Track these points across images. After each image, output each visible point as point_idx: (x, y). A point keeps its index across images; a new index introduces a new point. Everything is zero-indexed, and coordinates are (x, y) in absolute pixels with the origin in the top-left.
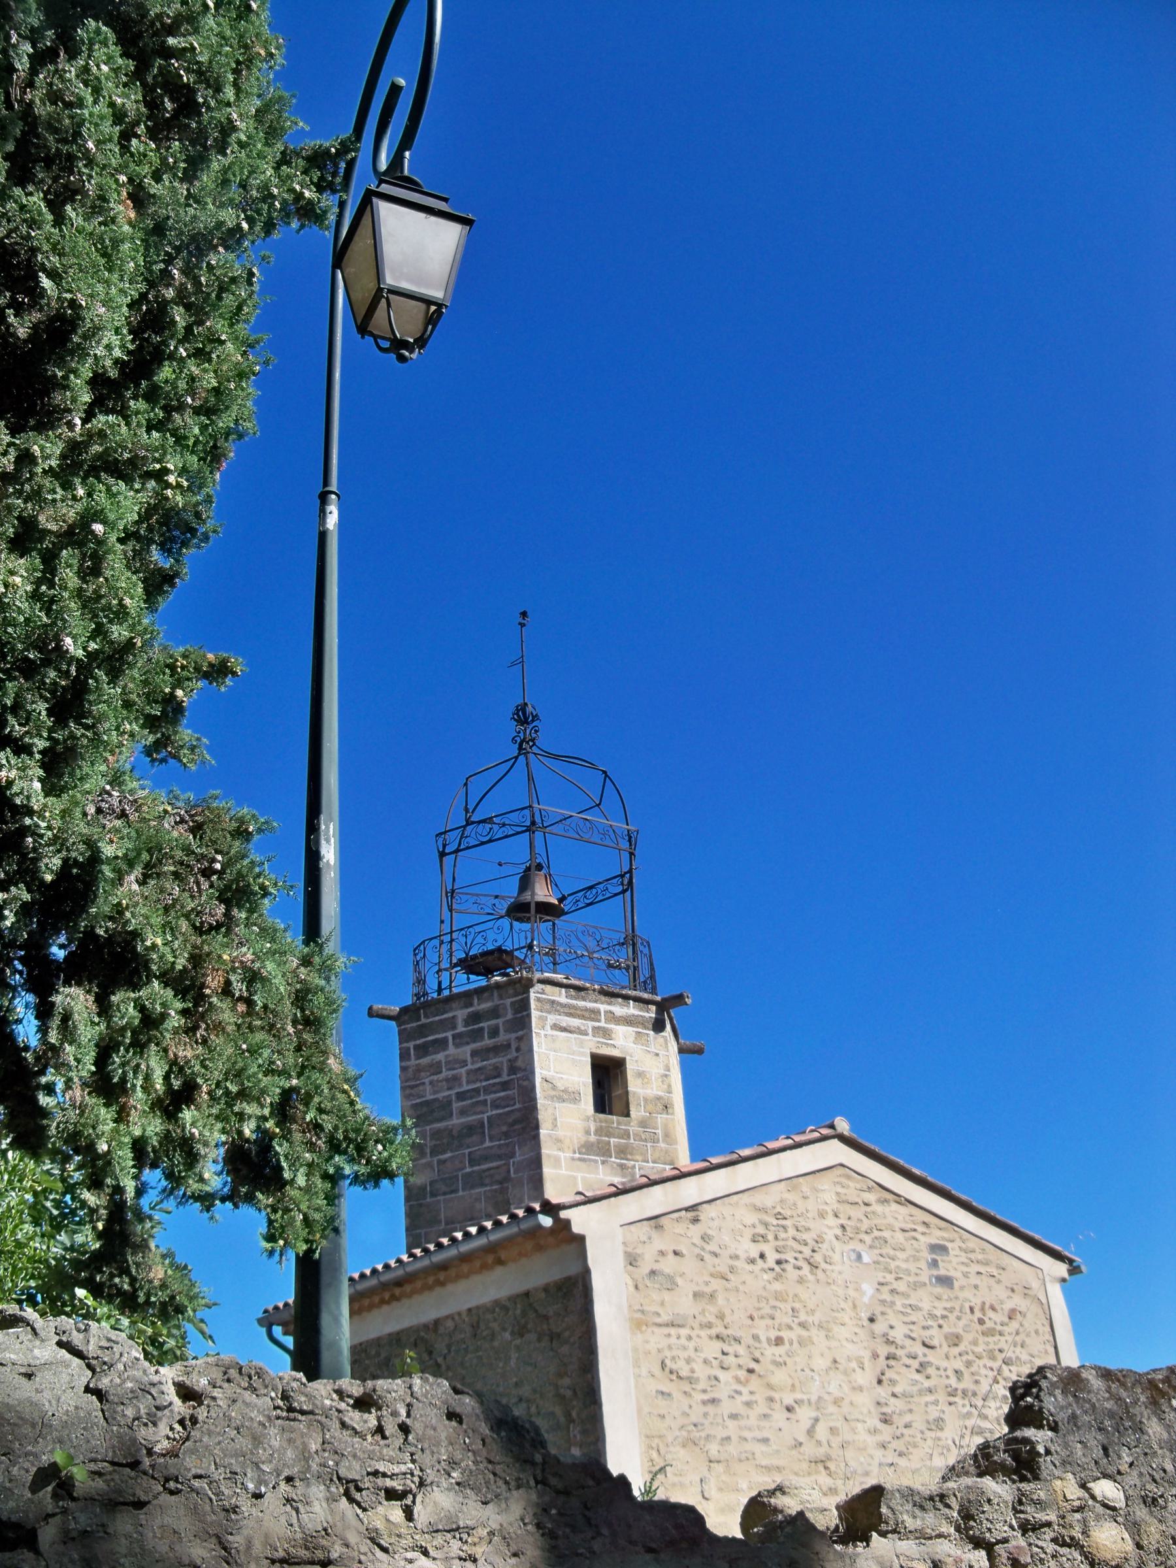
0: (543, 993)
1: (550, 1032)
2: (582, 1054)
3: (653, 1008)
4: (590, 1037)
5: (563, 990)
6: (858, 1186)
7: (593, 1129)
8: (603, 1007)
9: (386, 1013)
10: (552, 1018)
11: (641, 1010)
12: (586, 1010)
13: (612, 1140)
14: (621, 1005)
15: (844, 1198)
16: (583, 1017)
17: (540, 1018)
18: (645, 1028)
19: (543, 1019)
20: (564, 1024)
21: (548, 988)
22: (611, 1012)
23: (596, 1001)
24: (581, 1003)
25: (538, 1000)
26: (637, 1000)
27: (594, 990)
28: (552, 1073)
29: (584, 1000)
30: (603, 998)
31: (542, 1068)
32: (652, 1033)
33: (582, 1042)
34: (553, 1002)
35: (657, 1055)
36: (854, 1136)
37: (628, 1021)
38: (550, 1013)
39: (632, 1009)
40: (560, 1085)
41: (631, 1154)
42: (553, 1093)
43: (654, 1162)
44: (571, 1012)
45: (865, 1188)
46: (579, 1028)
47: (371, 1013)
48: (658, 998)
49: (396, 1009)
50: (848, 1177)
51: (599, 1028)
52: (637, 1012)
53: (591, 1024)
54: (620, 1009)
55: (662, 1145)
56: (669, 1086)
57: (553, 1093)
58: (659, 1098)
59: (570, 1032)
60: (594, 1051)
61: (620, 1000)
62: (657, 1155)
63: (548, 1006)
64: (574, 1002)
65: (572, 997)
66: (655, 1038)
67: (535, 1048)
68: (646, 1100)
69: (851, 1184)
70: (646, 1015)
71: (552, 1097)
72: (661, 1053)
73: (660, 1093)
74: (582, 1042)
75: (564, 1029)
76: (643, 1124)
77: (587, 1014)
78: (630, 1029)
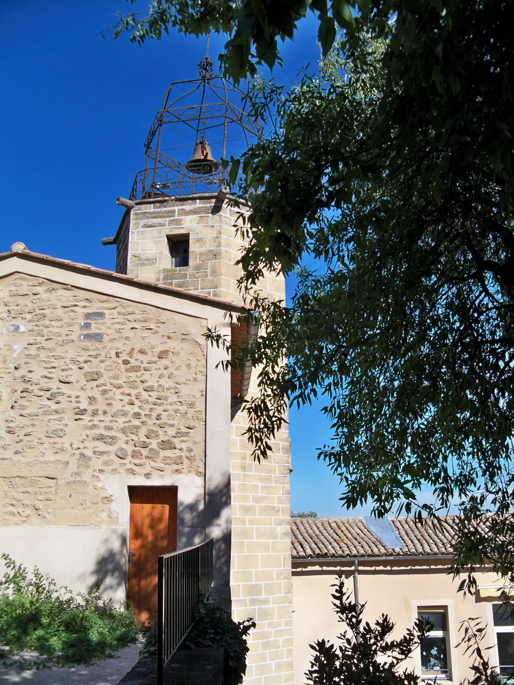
0: (140, 209)
1: (141, 229)
2: (162, 237)
3: (214, 200)
4: (167, 226)
5: (152, 205)
6: (31, 283)
7: (162, 277)
8: (176, 208)
9: (108, 241)
10: (142, 222)
11: (205, 203)
12: (166, 212)
13: (174, 281)
14: (190, 204)
15: (15, 293)
16: (161, 217)
17: (136, 224)
18: (206, 213)
19: (137, 224)
20: (150, 223)
21: (142, 207)
22: (183, 209)
23: (173, 206)
24: (163, 209)
25: (136, 214)
26: (201, 198)
27: (172, 200)
28: (139, 251)
29: (165, 207)
30: (178, 203)
31: (133, 250)
32: (211, 215)
33: (161, 230)
34: (145, 213)
35: (213, 226)
36: (27, 251)
37: (194, 212)
38: (141, 219)
39: (198, 204)
40: (144, 257)
41: (186, 287)
42: (139, 262)
43: (201, 289)
44: (155, 215)
45: (36, 284)
46: (160, 223)
47: (105, 244)
48: (216, 194)
49: (113, 238)
50: (23, 279)
51: (173, 220)
52: (201, 206)
53: (168, 219)
54: (188, 206)
55: (209, 278)
56: (219, 243)
57: (139, 262)
58: (210, 251)
59: (154, 227)
60: (168, 233)
61: (190, 201)
62: (205, 284)
63: (141, 216)
64: (159, 210)
65: (157, 207)
66: (213, 218)
67: (130, 240)
68: (201, 254)
69: (24, 283)
70: (208, 205)
71: (138, 264)
72: (215, 225)
73: (211, 248)
74: (161, 230)
75: (151, 226)
76: (197, 268)
77: (166, 215)
78: (196, 216)
